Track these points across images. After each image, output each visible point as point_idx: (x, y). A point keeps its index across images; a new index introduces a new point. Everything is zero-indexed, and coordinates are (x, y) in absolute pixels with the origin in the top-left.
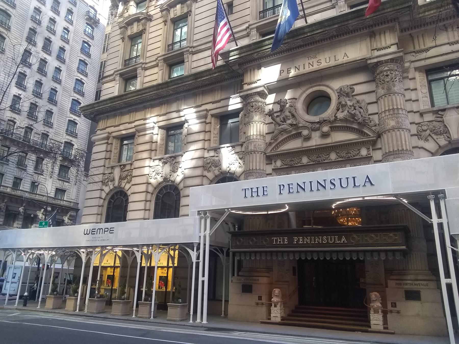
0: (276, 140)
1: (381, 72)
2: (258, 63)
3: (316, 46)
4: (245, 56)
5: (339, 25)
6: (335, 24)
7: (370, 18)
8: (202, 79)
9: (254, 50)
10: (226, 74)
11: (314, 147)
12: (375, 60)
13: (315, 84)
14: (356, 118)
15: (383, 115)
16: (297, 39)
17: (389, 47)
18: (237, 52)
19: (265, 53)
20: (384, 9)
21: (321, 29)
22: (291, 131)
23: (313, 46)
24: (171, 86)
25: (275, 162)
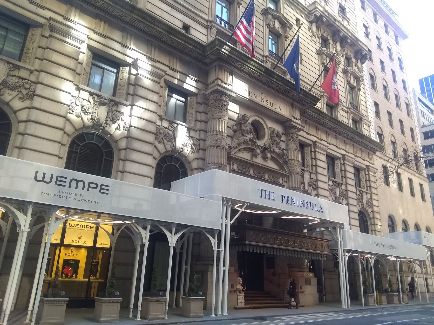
0: (239, 146)
1: (295, 133)
2: (232, 69)
3: (268, 88)
4: (234, 58)
5: (290, 89)
6: (288, 86)
7: (301, 97)
8: (175, 38)
9: (242, 59)
10: (199, 53)
11: (261, 165)
12: (295, 124)
13: (259, 115)
14: (284, 157)
15: (293, 162)
16: (268, 78)
17: (298, 120)
18: (229, 48)
19: (244, 67)
20: (308, 97)
21: (281, 82)
22: (249, 145)
23: (266, 88)
24: (135, 14)
25: (233, 164)
